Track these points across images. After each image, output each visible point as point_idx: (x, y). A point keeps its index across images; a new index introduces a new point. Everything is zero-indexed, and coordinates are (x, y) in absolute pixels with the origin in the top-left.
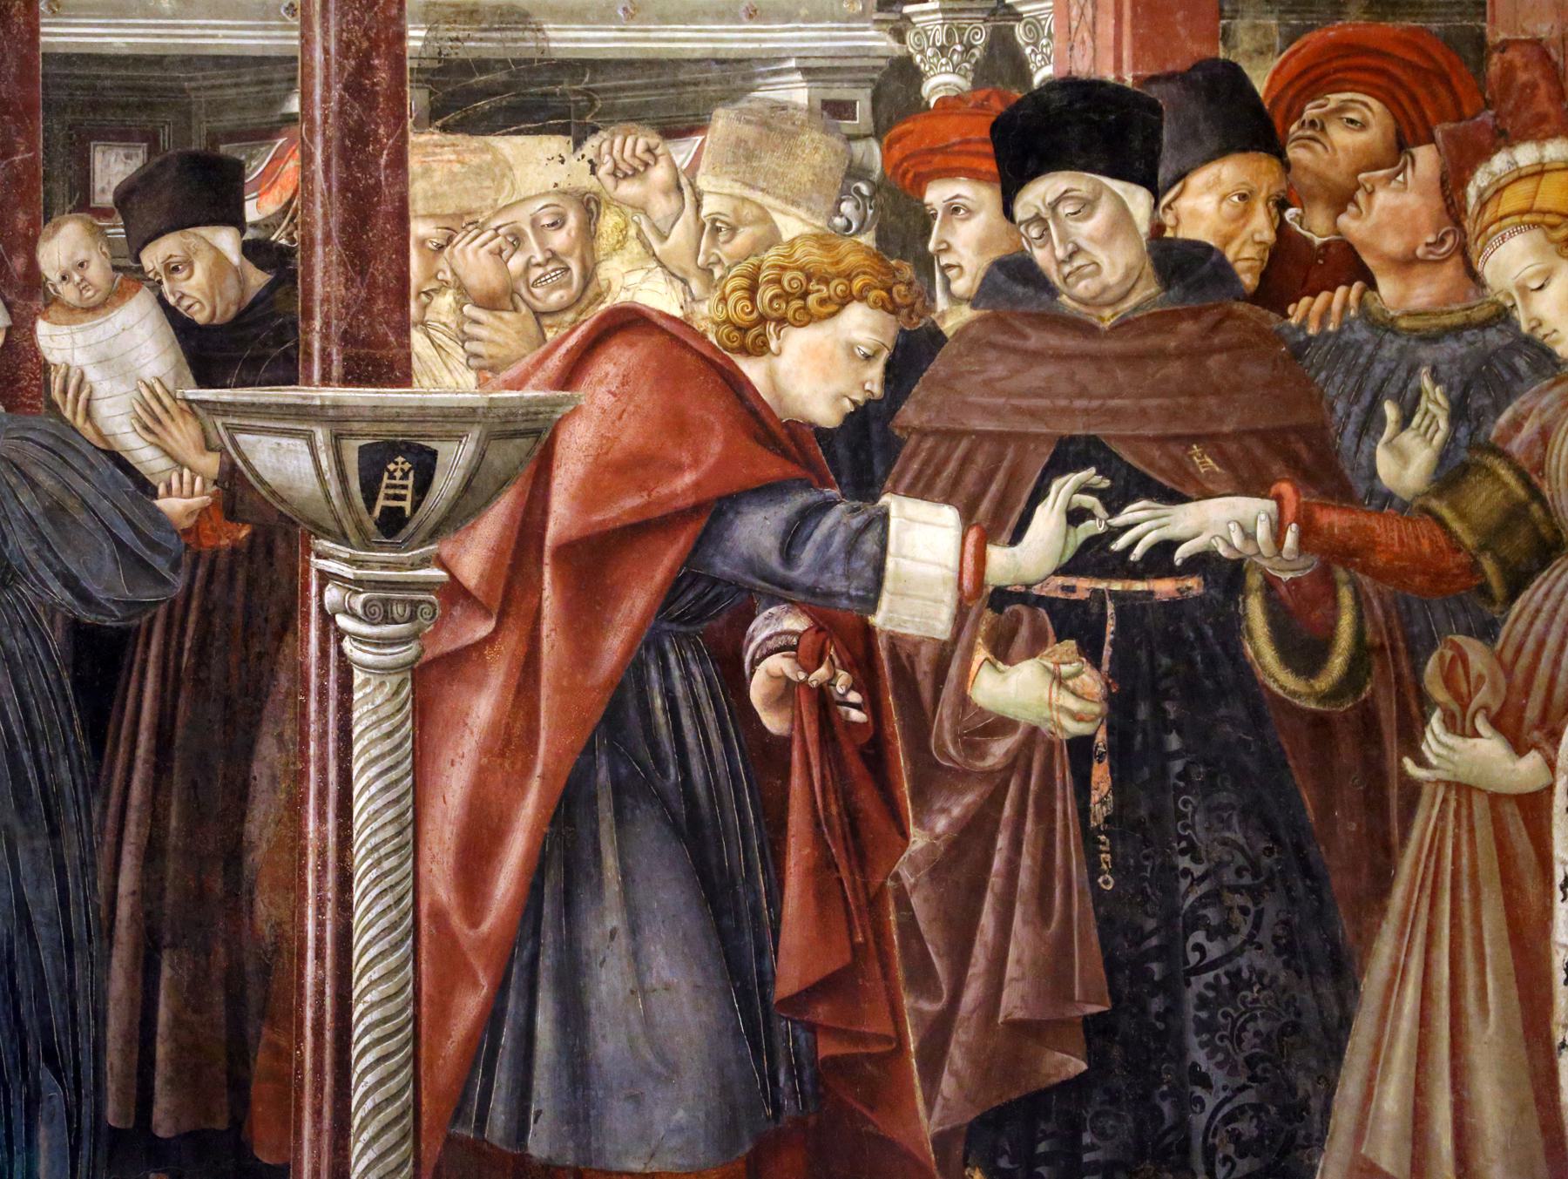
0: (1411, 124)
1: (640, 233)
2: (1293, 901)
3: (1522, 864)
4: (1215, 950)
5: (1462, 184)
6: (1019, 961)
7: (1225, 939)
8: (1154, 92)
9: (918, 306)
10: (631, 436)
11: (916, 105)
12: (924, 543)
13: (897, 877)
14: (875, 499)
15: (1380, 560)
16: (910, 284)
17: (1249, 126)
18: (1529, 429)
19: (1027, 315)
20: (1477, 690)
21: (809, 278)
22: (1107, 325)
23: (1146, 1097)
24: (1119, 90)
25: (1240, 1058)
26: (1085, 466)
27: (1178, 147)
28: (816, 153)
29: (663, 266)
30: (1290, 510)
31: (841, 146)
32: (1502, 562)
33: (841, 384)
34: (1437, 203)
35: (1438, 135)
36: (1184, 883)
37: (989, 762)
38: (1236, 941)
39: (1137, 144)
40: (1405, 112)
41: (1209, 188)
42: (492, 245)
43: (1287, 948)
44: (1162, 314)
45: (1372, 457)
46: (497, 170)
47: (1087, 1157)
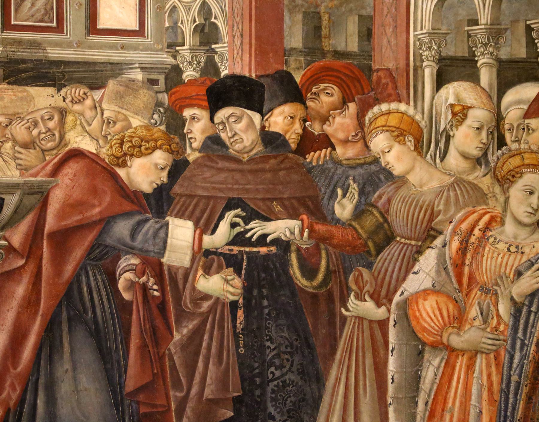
0: (347, 95)
1: (81, 123)
2: (304, 357)
3: (379, 343)
4: (278, 373)
5: (364, 116)
6: (211, 378)
7: (281, 370)
8: (262, 80)
9: (180, 152)
10: (77, 194)
11: (181, 82)
12: (181, 233)
13: (169, 350)
14: (164, 218)
15: (335, 242)
16: (177, 144)
17: (294, 94)
18: (384, 198)
19: (218, 156)
20: (366, 285)
21: (142, 141)
22: (245, 160)
24: (250, 79)
25: (285, 410)
26: (237, 208)
27: (270, 100)
28: (145, 97)
29: (89, 134)
30: (306, 225)
31: (153, 95)
32: (374, 243)
33: (152, 178)
34: (356, 122)
35: (356, 99)
36: (268, 351)
37: (202, 310)
38: (285, 370)
39: (256, 98)
40: (345, 91)
41: (280, 114)
42: (26, 125)
43: (302, 373)
44: (264, 157)
46: (28, 99)
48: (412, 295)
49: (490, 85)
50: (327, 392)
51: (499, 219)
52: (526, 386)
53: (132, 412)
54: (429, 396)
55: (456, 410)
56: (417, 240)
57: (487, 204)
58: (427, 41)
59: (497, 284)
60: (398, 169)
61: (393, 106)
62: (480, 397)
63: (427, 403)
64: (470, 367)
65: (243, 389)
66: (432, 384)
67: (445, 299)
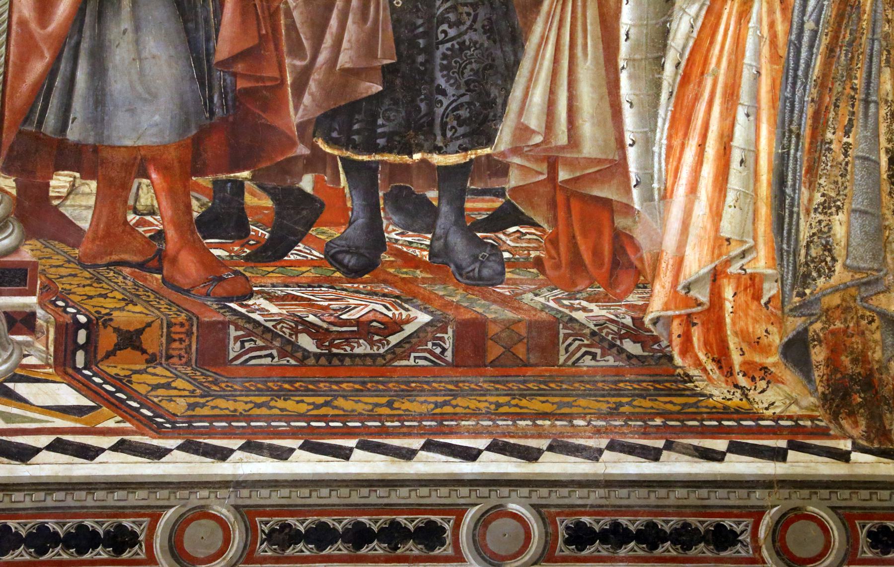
2: (492, 8)
4: (452, 32)
6: (349, 41)
7: (458, 27)
23: (413, 100)
38: (463, 28)
43: (490, 30)
47: (379, 130)
50: (527, 56)
52: (826, 35)
53: (225, 88)
54: (681, 55)
62: (758, 54)
63: (678, 65)
65: (399, 54)
66: (687, 39)
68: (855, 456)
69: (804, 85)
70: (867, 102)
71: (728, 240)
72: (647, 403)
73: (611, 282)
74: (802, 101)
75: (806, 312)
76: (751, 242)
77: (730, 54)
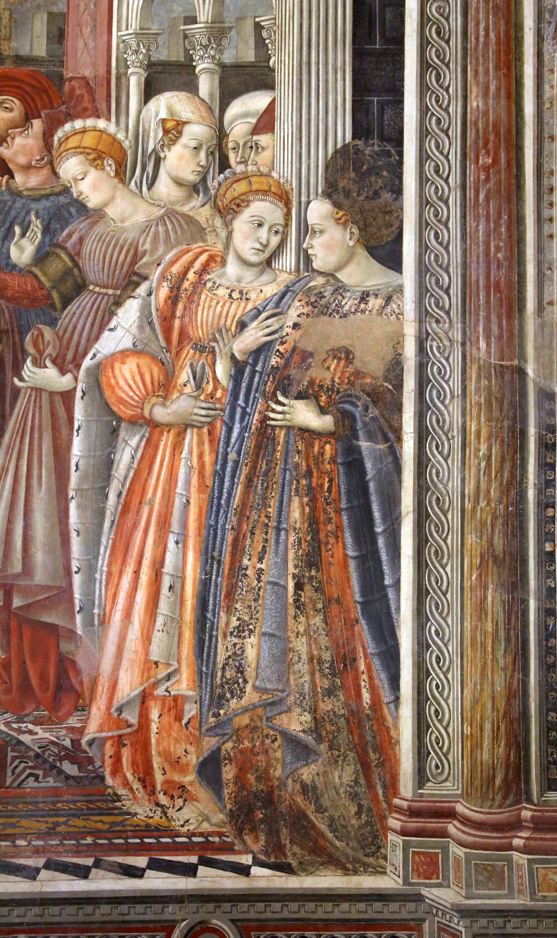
3: (61, 421)
5: (52, 136)
15: (9, 293)
18: (75, 237)
20: (47, 347)
32: (60, 293)
34: (41, 143)
35: (43, 115)
45: (9, 249)
48: (106, 358)
49: (211, 95)
51: (218, 259)
52: (246, 466)
54: (123, 485)
55: (157, 500)
56: (116, 288)
57: (204, 241)
58: (133, 43)
59: (215, 340)
60: (93, 200)
61: (90, 122)
62: (188, 483)
63: (119, 495)
64: (177, 446)
66: (128, 470)
67: (149, 361)
68: (256, 870)
69: (226, 513)
70: (278, 530)
71: (156, 663)
72: (80, 823)
73: (54, 705)
74: (224, 529)
75: (219, 731)
76: (175, 665)
77: (165, 483)
